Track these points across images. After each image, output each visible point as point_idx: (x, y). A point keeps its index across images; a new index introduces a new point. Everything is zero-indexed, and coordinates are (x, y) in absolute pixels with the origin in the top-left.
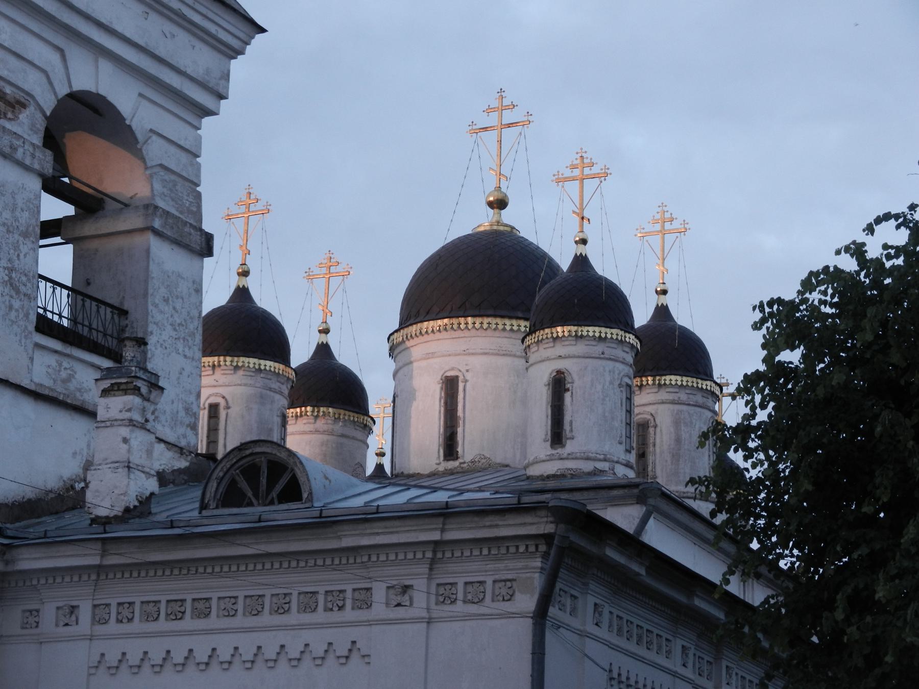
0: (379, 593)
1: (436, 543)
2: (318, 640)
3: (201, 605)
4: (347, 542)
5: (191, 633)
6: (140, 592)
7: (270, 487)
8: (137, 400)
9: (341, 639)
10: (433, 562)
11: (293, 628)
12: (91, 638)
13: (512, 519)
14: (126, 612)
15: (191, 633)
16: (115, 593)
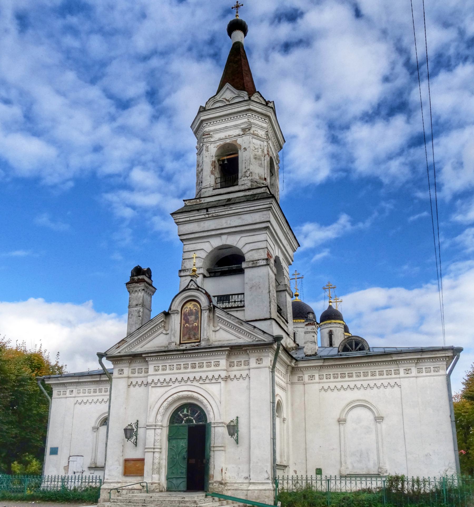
0: (402, 370)
1: (418, 359)
2: (385, 382)
3: (350, 375)
4: (394, 359)
5: (355, 381)
6: (331, 372)
7: (356, 348)
8: (314, 326)
9: (392, 382)
10: (416, 363)
11: (378, 379)
12: (319, 383)
13: (441, 352)
14: (328, 377)
15: (355, 381)
16: (325, 372)
